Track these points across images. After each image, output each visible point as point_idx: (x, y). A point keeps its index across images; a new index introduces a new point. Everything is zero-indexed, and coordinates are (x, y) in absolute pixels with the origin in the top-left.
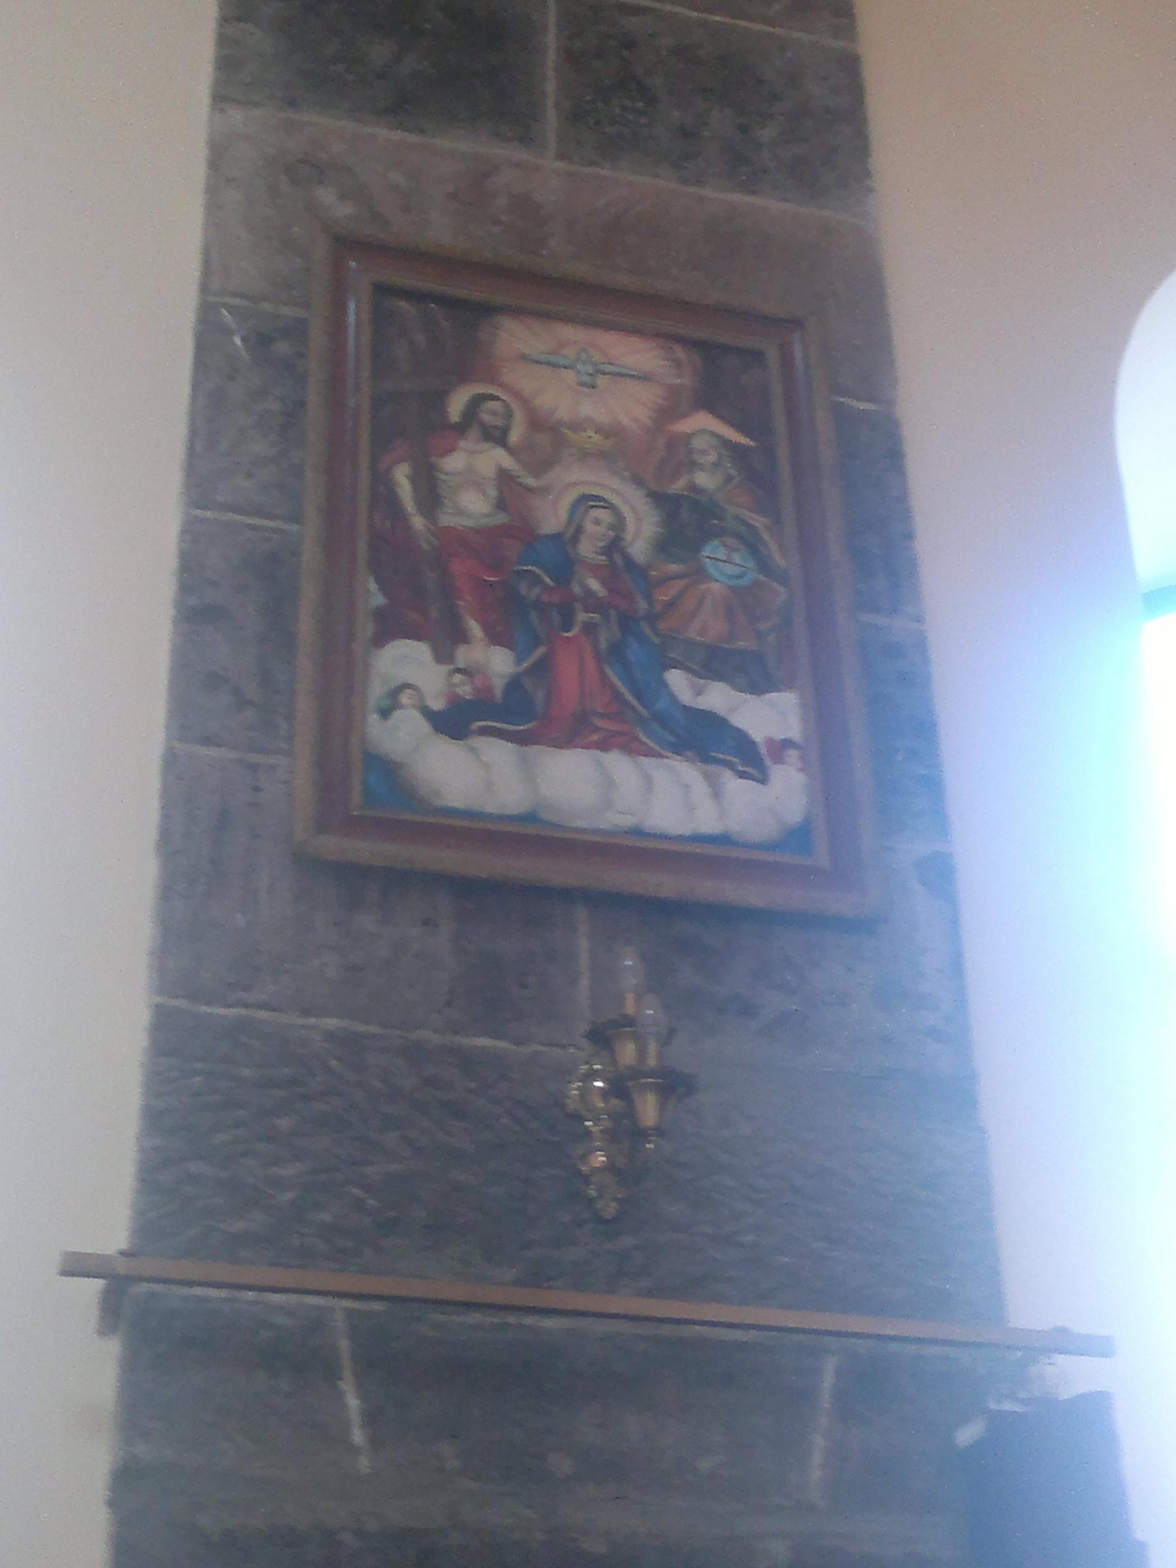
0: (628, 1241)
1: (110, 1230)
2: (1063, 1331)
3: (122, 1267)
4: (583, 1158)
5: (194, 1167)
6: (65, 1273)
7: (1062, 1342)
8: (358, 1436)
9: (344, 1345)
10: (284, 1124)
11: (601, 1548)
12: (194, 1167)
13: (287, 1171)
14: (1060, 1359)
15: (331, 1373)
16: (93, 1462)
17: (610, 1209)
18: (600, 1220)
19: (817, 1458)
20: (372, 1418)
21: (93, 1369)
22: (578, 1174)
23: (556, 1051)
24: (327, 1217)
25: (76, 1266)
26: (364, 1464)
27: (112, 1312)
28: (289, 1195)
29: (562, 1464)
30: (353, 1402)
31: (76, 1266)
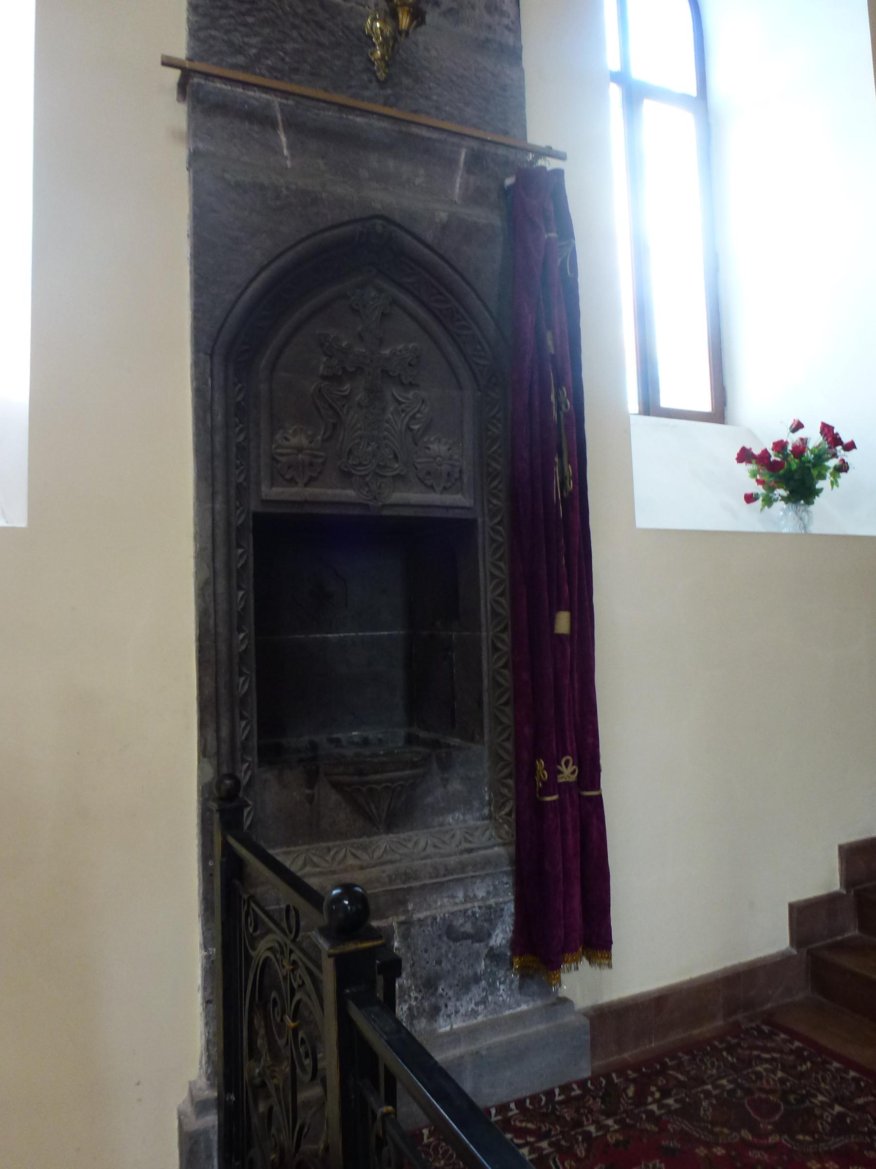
0: (389, 91)
1: (181, 52)
2: (550, 148)
3: (188, 65)
4: (372, 54)
5: (213, 32)
6: (164, 64)
7: (549, 153)
8: (286, 152)
9: (279, 117)
10: (250, 20)
11: (379, 206)
12: (213, 32)
13: (254, 41)
14: (548, 159)
15: (274, 125)
16: (180, 154)
17: (381, 75)
18: (378, 81)
19: (458, 185)
20: (290, 147)
21: (177, 115)
22: (370, 60)
23: (361, 8)
24: (270, 63)
25: (168, 63)
26: (289, 164)
27: (183, 87)
28: (254, 51)
29: (364, 173)
30: (283, 139)
31: (168, 63)
